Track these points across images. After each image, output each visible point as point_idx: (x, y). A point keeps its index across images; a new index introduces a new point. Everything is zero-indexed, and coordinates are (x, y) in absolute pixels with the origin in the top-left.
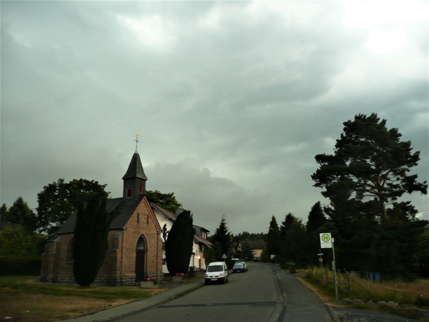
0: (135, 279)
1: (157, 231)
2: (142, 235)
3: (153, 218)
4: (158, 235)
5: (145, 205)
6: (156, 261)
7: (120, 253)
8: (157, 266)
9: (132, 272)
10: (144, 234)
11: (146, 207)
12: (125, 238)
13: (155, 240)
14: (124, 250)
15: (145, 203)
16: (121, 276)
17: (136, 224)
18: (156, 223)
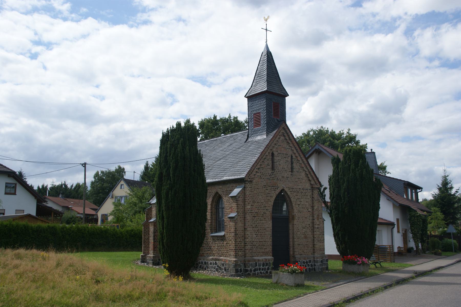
0: (272, 266)
1: (311, 184)
2: (283, 190)
3: (301, 162)
4: (313, 191)
5: (285, 139)
6: (311, 236)
7: (241, 221)
8: (314, 245)
9: (266, 254)
10: (286, 190)
11: (288, 142)
12: (249, 196)
13: (308, 199)
14: (248, 217)
15: (284, 136)
16: (245, 261)
17: (270, 172)
18: (308, 170)
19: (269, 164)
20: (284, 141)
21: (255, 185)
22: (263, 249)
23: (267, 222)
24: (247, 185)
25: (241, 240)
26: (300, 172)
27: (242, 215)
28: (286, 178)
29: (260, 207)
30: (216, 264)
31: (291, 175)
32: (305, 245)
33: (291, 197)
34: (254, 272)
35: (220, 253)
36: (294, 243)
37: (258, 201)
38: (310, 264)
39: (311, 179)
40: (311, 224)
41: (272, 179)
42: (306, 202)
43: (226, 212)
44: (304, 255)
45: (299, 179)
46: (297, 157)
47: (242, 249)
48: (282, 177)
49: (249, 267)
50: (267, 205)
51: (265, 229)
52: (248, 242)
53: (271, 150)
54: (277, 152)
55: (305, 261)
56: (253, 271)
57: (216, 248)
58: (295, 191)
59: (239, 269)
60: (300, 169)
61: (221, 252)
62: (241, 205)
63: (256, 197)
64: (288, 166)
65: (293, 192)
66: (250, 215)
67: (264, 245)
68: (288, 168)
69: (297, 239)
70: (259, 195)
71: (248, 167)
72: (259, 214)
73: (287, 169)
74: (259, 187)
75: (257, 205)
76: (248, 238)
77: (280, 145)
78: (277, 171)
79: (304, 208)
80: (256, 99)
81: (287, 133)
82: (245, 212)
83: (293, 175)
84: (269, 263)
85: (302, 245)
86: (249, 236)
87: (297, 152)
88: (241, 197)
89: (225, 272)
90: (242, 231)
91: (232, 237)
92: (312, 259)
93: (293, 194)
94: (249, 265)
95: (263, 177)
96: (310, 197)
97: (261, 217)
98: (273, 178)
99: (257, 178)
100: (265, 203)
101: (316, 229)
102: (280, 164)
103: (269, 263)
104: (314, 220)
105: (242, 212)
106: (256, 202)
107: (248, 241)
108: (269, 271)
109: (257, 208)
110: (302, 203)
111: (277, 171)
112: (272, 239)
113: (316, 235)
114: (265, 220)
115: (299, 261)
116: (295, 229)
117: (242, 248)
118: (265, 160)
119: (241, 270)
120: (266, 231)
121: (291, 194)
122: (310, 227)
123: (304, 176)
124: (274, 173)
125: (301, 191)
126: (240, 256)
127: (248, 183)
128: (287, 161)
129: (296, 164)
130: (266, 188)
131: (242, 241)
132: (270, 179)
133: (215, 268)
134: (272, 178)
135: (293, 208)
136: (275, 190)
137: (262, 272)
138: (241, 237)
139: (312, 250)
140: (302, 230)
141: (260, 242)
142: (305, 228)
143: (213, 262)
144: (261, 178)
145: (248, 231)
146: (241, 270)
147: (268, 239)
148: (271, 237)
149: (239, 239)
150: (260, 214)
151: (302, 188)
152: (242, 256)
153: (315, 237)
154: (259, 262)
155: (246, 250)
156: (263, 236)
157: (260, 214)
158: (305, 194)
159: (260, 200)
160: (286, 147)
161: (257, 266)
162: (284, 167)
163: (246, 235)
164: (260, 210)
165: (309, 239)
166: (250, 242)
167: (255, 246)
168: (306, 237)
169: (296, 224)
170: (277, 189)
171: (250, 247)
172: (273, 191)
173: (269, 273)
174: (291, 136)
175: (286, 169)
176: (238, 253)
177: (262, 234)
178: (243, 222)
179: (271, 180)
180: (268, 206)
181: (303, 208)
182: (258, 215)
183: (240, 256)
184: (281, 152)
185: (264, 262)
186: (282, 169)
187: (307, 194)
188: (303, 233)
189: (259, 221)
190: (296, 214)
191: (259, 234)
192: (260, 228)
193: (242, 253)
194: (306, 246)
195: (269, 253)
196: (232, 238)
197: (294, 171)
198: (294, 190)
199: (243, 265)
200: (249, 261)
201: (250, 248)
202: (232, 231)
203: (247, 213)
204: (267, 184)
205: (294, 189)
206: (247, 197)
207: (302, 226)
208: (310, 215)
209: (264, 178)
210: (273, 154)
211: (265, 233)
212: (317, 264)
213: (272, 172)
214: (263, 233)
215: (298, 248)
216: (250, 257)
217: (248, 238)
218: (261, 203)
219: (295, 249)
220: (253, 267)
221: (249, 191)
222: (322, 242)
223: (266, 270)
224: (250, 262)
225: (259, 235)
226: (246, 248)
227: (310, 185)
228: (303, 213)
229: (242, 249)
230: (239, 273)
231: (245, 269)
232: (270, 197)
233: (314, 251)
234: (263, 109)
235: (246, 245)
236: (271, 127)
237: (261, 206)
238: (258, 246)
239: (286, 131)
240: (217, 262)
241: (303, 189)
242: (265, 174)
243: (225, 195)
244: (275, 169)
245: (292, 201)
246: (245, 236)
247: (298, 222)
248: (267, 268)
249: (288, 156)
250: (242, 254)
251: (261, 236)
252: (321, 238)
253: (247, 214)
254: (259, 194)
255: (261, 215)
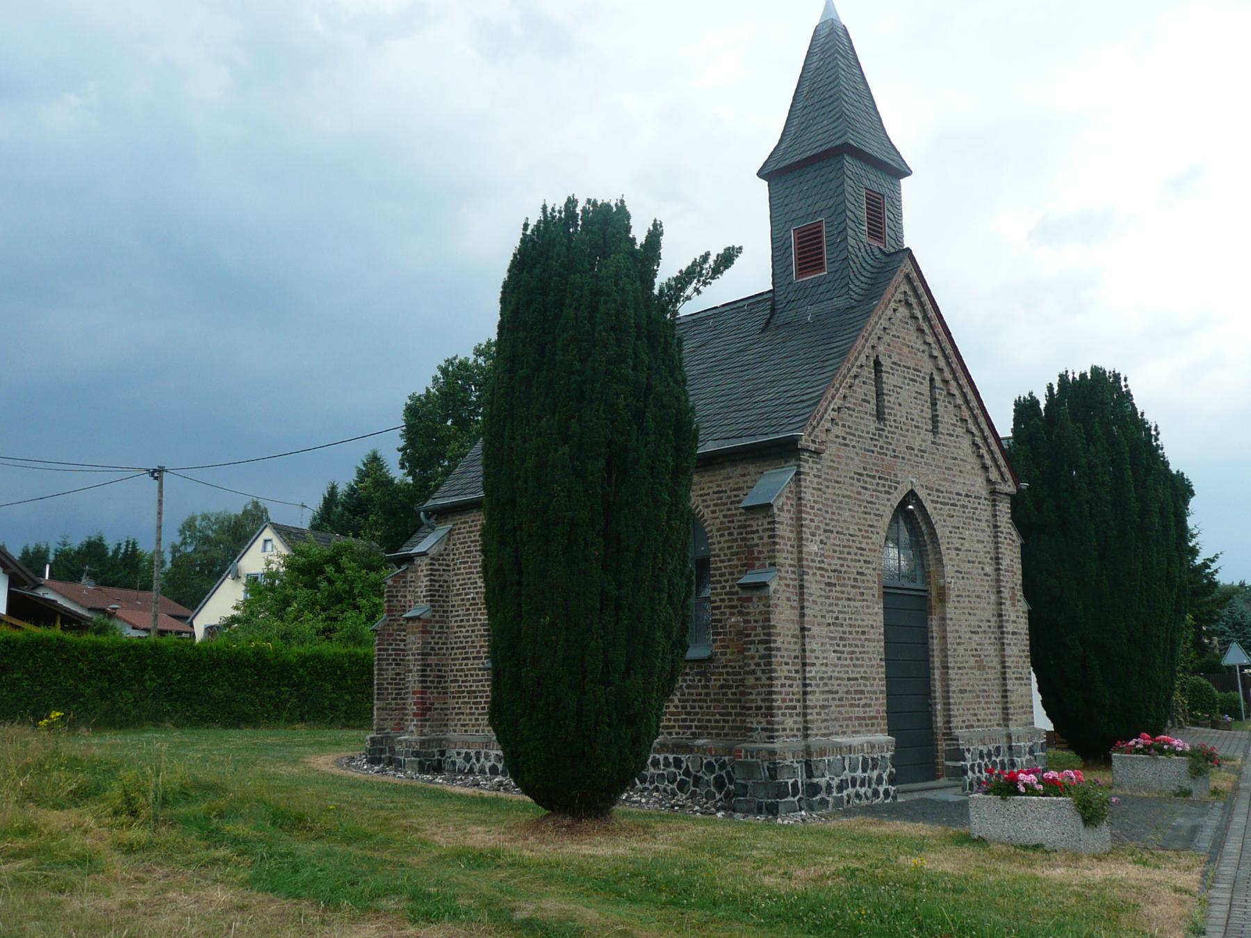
0: (890, 769)
1: (989, 481)
2: (912, 494)
3: (960, 401)
4: (994, 506)
5: (914, 318)
6: (996, 662)
7: (788, 599)
8: (1005, 694)
9: (867, 723)
10: (922, 494)
11: (921, 330)
12: (812, 508)
13: (983, 531)
14: (814, 586)
15: (908, 305)
16: (808, 751)
17: (872, 425)
18: (982, 431)
19: (868, 398)
20: (907, 323)
21: (830, 467)
22: (858, 706)
23: (868, 607)
24: (807, 465)
25: (790, 671)
26: (957, 437)
27: (793, 576)
28: (919, 454)
29: (846, 550)
30: (678, 763)
31: (933, 443)
32: (981, 694)
33: (936, 523)
34: (838, 792)
35: (696, 723)
36: (948, 685)
37: (841, 530)
38: (998, 760)
39: (988, 462)
40: (995, 618)
41: (879, 453)
42: (978, 541)
43: (716, 569)
44: (978, 727)
45: (955, 459)
46: (945, 382)
47: (795, 708)
48: (907, 447)
49: (823, 776)
50: (867, 544)
51: (863, 633)
52: (815, 678)
53: (873, 347)
54: (890, 357)
55: (985, 751)
56: (834, 790)
57: (676, 707)
58: (947, 501)
59: (791, 781)
60: (955, 425)
61: (700, 720)
62: (789, 539)
63: (833, 513)
64: (922, 411)
65: (941, 503)
66: (818, 578)
67: (862, 692)
68: (922, 417)
69: (955, 671)
70: (843, 506)
71: (802, 401)
72: (842, 575)
73: (920, 420)
74: (840, 476)
75: (837, 542)
76: (814, 664)
77: (899, 337)
78: (892, 423)
79: (973, 562)
80: (801, 179)
81: (918, 296)
82: (802, 566)
83: (939, 445)
84: (882, 757)
85: (970, 691)
86: (816, 658)
87: (949, 364)
88: (785, 508)
89: (718, 797)
90: (792, 637)
91: (757, 660)
92: (1003, 744)
93: (941, 509)
94: (821, 766)
95: (854, 443)
96: (989, 526)
97: (849, 589)
98: (882, 448)
99: (835, 443)
100: (860, 538)
101: (1010, 636)
102: (900, 400)
103: (882, 757)
104: (1003, 607)
105: (791, 566)
106: (835, 530)
107: (813, 674)
108: (881, 789)
109: (837, 555)
110: (967, 546)
111: (892, 423)
112: (884, 669)
113: (1011, 659)
114: (863, 600)
115: (968, 750)
116: (949, 635)
117: (794, 703)
118: (857, 380)
119: (795, 785)
120: (866, 639)
121: (935, 508)
122: (992, 630)
123: (970, 451)
124: (883, 430)
125: (962, 503)
126: (788, 732)
127: (811, 460)
128: (920, 394)
129: (946, 407)
130: (861, 484)
131: (793, 675)
132: (873, 452)
133: (675, 780)
134: (878, 449)
135: (940, 561)
136: (889, 493)
137: (862, 791)
138: (790, 661)
139: (1000, 711)
140: (970, 638)
141: (849, 679)
142: (978, 633)
143: (666, 759)
144: (846, 445)
145: (814, 637)
146: (795, 785)
147: (874, 670)
148: (883, 663)
149: (785, 668)
150: (846, 576)
151: (964, 493)
152: (795, 732)
153: (1007, 664)
154: (852, 756)
155: (809, 711)
156: (858, 659)
157: (846, 576)
158: (974, 513)
159: (847, 525)
160: (914, 345)
161: (847, 771)
162: (911, 414)
163: (808, 654)
164: (845, 563)
165: (989, 671)
166: (822, 679)
167: (834, 696)
168: (981, 666)
169: (951, 619)
170: (896, 488)
171: (822, 697)
172: (883, 495)
173: (882, 795)
174: (929, 306)
175: (918, 422)
176: (783, 723)
177: (856, 649)
178: (795, 604)
179: (876, 454)
180: (870, 550)
181: (969, 562)
182: (842, 582)
183: (788, 732)
184: (900, 360)
185: (867, 756)
186: (907, 419)
187: (979, 515)
188: (972, 650)
189: (846, 603)
190: (950, 583)
191: (847, 649)
192: (847, 629)
193: (795, 722)
194: (983, 697)
195: (879, 720)
196: (758, 665)
197: (940, 429)
198: (944, 497)
199: (801, 767)
200: (822, 752)
201: (821, 703)
202: (756, 639)
203: (811, 572)
204: (865, 469)
205: (942, 492)
206: (808, 510)
207: (970, 626)
208: (990, 586)
209: (854, 447)
210: (877, 364)
211: (863, 646)
212: (1019, 760)
213: (877, 425)
214: (857, 646)
215: (960, 704)
216: (824, 735)
217: (814, 664)
218: (848, 537)
219: (951, 707)
220: (837, 776)
221: (814, 489)
222: (1025, 681)
223: (874, 786)
224: (825, 755)
225: (845, 655)
226: (808, 703)
227: (985, 483)
228: (971, 581)
229: (795, 708)
230: (790, 799)
231: (808, 781)
232: (876, 515)
233: (1007, 714)
234: (833, 209)
235: (809, 689)
236: (865, 273)
237: (849, 547)
238: (845, 695)
239: (915, 290)
240: (683, 757)
241: (967, 496)
242: (857, 433)
243: (712, 508)
244: (886, 416)
245: (939, 536)
246: (804, 657)
247: (957, 612)
248: (875, 777)
249: (921, 375)
250: (796, 726)
251: (852, 659)
252: (1023, 668)
253: (808, 574)
254: (841, 502)
255: (849, 579)
